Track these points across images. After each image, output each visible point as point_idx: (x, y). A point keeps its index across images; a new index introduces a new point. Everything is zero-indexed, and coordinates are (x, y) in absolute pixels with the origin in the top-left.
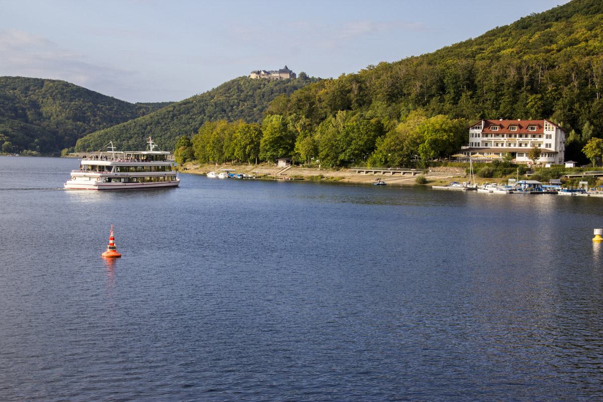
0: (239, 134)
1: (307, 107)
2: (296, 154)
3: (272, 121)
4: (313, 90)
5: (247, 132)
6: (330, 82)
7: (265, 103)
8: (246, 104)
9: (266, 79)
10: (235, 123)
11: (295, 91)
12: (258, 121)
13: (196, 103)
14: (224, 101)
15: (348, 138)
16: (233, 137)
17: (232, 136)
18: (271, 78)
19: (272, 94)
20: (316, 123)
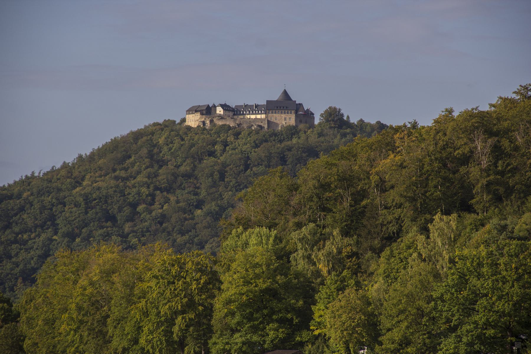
0: (153, 284)
1: (346, 204)
2: (317, 337)
3: (246, 244)
4: (363, 157)
5: (178, 277)
6: (410, 134)
7: (227, 195)
8: (173, 198)
9: (229, 128)
10: (142, 253)
11: (311, 160)
12: (208, 246)
13: (31, 198)
14: (111, 191)
15: (465, 293)
16: (136, 291)
17: (132, 288)
18: (245, 126)
19: (246, 170)
20: (373, 249)
